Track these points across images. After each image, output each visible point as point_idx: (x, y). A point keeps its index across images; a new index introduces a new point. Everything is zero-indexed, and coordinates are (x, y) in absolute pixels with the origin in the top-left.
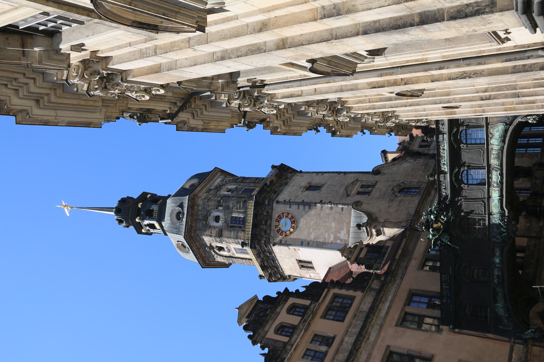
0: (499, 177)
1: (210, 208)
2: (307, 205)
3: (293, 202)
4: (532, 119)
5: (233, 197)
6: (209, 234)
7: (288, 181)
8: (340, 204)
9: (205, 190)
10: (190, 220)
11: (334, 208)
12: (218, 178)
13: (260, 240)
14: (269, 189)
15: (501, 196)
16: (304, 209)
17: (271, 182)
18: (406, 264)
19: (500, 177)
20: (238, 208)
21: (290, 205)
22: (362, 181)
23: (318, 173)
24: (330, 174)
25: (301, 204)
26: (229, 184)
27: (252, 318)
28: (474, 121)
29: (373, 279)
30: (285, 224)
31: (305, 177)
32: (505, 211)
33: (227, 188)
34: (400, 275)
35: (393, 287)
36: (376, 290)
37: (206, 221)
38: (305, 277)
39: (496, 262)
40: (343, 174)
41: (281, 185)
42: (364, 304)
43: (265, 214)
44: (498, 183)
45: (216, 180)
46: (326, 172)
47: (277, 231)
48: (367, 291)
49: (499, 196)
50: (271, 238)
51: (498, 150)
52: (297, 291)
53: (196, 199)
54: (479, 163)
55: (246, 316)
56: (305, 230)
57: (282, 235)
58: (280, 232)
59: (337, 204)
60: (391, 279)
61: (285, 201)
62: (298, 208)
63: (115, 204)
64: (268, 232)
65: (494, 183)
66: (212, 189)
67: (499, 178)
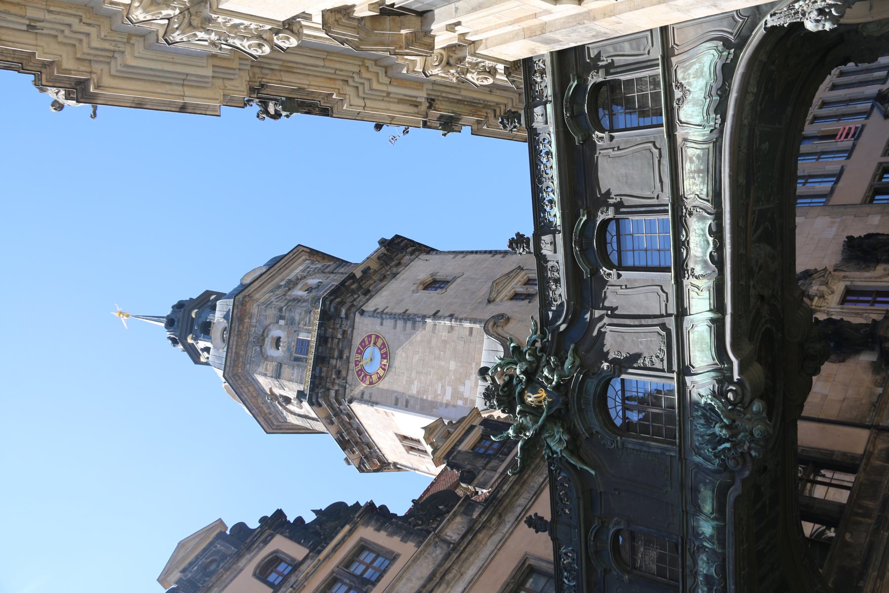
0: (711, 239)
1: (268, 322)
2: (409, 320)
3: (386, 313)
4: (814, 15)
5: (305, 301)
6: (263, 371)
7: (400, 270)
8: (466, 319)
9: (270, 286)
10: (235, 343)
11: (456, 328)
12: (300, 265)
13: (329, 390)
14: (354, 286)
15: (719, 307)
16: (405, 329)
17: (366, 271)
18: (542, 480)
19: (714, 242)
20: (307, 322)
21: (382, 319)
22: (531, 270)
23: (456, 253)
24: (478, 256)
25: (400, 319)
26: (313, 277)
27: (190, 575)
28: (627, 49)
29: (455, 512)
30: (372, 360)
31: (431, 261)
32: (731, 363)
33: (306, 284)
34: (519, 509)
35: (489, 543)
36: (449, 543)
37: (261, 347)
38: (420, 469)
39: (703, 533)
40: (502, 255)
41: (384, 278)
42: (409, 580)
43: (339, 336)
44: (705, 262)
45: (296, 268)
46: (472, 252)
47: (357, 372)
48: (427, 546)
49: (710, 310)
50: (347, 386)
51: (704, 142)
52: (300, 520)
53: (248, 304)
54: (648, 194)
55: (182, 567)
56: (404, 373)
57: (364, 382)
59: (461, 320)
60: (489, 520)
61: (375, 311)
62: (395, 327)
63: (168, 311)
64: (344, 373)
65: (696, 263)
66: (281, 286)
67: (708, 243)
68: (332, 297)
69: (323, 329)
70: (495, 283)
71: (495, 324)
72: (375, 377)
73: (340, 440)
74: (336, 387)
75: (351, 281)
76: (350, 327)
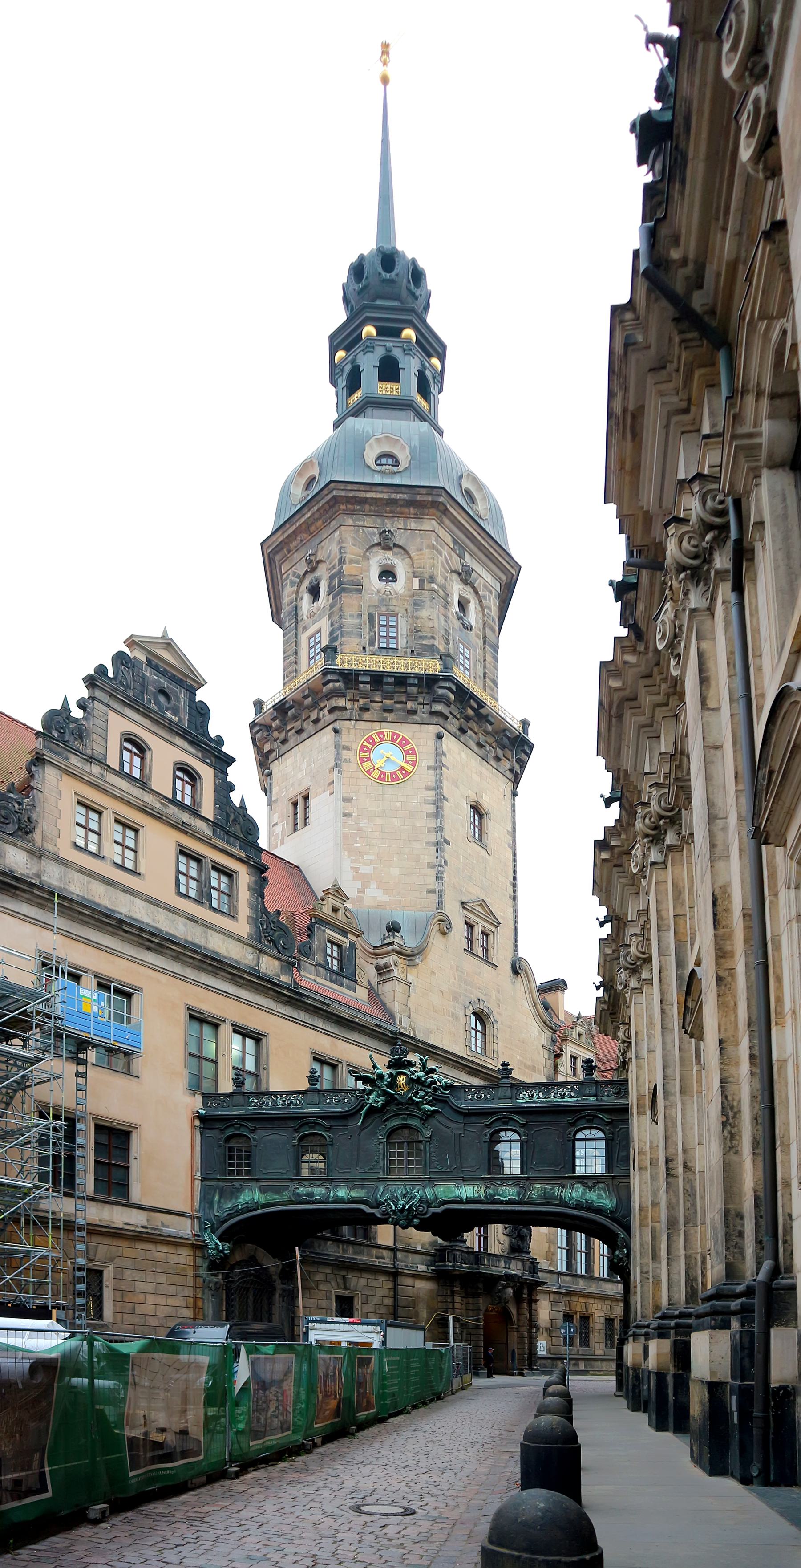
14: (470, 712)
43: (410, 705)
52: (231, 787)
58: (370, 746)
61: (443, 754)
68: (454, 688)
69: (416, 681)
70: (483, 904)
71: (441, 921)
72: (367, 765)
73: (284, 704)
74: (349, 705)
75: (476, 706)
76: (422, 718)
